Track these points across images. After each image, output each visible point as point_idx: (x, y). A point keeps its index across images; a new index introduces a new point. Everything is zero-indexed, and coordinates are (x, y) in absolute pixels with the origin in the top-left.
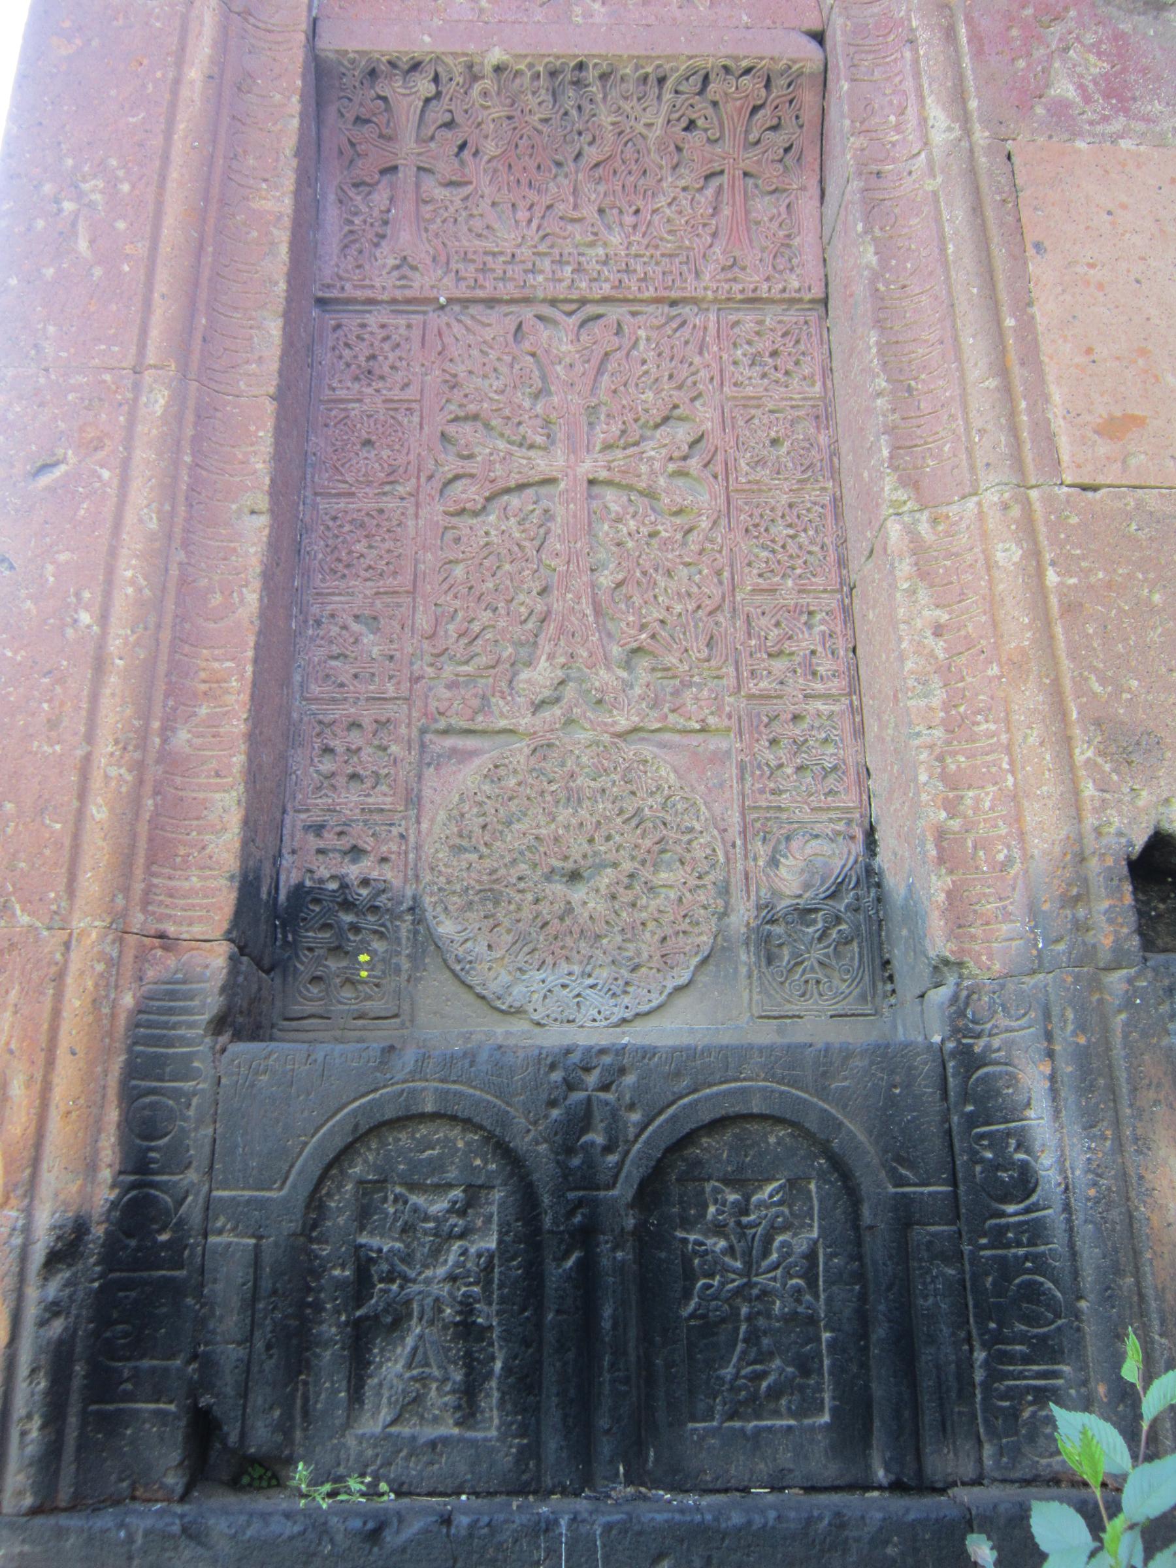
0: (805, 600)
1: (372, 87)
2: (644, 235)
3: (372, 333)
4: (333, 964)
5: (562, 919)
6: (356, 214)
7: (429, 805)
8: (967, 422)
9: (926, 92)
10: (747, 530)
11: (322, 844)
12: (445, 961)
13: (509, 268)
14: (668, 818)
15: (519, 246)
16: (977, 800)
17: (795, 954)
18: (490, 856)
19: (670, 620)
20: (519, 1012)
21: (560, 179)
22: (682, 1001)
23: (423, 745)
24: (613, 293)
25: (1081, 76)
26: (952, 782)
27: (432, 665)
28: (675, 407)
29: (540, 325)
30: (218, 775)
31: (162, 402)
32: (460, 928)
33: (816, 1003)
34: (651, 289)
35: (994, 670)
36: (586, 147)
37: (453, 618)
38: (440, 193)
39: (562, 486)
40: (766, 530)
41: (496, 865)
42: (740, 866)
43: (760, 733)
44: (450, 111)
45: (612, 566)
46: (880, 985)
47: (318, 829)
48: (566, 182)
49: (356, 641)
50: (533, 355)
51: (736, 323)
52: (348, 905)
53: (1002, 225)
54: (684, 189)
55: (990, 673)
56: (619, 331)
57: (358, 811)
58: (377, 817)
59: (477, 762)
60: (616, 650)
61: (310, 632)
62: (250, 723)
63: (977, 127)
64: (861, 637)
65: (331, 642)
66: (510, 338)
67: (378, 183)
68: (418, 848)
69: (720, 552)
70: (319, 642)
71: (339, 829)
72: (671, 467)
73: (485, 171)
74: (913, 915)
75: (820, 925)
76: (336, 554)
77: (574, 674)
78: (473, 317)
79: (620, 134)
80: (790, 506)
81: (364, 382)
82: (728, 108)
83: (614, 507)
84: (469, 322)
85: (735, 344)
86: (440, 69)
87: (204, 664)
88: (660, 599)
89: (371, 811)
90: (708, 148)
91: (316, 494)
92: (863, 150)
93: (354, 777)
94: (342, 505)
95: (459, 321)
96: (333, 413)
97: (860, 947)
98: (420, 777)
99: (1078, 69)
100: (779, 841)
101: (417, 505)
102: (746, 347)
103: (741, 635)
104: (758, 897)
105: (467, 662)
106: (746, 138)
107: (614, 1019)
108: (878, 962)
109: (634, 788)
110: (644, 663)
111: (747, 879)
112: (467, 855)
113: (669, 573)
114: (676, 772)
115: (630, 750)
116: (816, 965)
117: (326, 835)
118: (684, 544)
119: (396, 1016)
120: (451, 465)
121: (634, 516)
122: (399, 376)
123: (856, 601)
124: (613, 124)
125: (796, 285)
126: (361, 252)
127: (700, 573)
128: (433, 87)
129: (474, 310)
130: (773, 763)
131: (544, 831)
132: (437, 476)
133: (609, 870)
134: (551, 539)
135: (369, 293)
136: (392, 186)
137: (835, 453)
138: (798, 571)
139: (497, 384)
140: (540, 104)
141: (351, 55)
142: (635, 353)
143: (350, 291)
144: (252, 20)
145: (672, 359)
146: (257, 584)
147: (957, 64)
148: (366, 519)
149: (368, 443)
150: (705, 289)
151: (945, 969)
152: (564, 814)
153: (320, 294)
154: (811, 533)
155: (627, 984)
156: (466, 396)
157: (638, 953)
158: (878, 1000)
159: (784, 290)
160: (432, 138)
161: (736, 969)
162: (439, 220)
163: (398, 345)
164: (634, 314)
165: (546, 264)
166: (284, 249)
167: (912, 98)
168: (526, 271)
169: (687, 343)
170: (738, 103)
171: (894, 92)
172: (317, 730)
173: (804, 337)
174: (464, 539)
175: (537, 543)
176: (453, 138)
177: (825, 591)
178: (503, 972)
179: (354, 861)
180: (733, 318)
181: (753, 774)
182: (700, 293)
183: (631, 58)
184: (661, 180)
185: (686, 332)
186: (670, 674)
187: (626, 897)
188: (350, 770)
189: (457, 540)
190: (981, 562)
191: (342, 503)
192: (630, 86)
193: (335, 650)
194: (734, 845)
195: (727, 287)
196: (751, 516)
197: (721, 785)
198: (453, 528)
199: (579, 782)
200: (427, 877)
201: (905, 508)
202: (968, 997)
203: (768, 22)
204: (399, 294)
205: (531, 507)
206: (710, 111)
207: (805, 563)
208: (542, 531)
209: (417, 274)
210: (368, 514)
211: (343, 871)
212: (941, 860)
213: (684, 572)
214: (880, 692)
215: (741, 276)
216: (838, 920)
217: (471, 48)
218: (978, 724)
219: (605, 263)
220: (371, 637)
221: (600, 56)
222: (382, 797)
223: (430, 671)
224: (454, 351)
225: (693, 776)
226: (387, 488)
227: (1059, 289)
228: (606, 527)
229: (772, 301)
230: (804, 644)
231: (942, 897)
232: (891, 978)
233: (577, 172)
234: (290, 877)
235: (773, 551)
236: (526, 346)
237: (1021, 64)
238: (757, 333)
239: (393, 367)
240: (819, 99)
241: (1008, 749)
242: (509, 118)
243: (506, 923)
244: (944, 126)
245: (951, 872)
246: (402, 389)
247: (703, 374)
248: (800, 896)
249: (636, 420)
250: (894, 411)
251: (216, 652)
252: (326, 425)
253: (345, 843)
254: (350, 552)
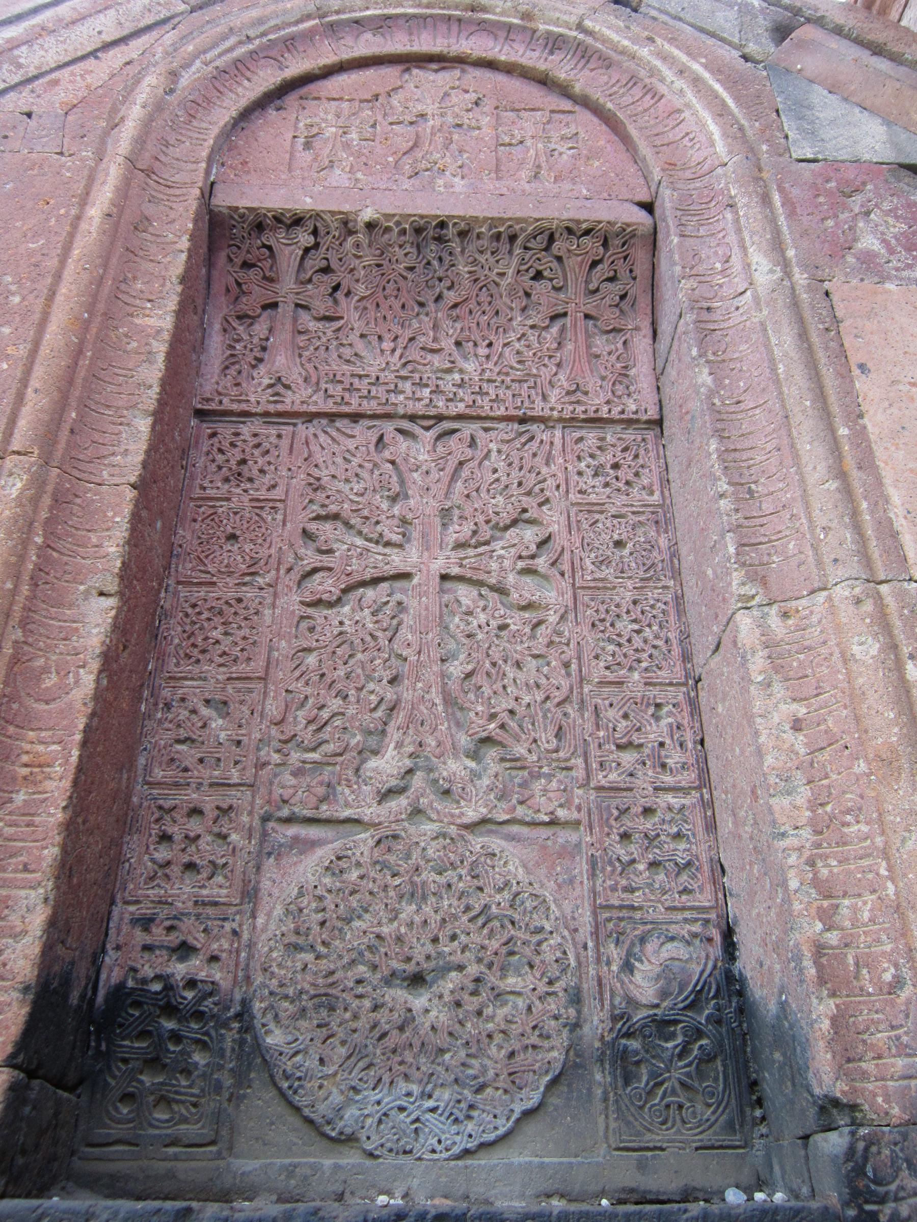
0: (652, 692)
1: (259, 238)
2: (495, 364)
3: (244, 441)
4: (147, 1079)
5: (401, 1029)
6: (238, 341)
7: (266, 899)
8: (810, 520)
9: (748, 244)
10: (593, 625)
11: (148, 940)
12: (272, 1077)
13: (373, 389)
14: (516, 917)
15: (383, 370)
16: (855, 910)
17: (653, 1075)
18: (326, 956)
19: (521, 710)
20: (348, 1140)
21: (422, 316)
22: (531, 1128)
23: (265, 834)
24: (467, 411)
25: (883, 233)
26: (825, 888)
27: (278, 751)
28: (525, 511)
29: (400, 438)
30: (26, 869)
31: (19, 485)
32: (290, 1038)
33: (679, 1132)
34: (503, 409)
35: (861, 767)
36: (445, 291)
37: (302, 705)
38: (312, 325)
39: (415, 581)
40: (612, 625)
41: (332, 967)
42: (592, 972)
43: (611, 827)
44: (327, 259)
45: (462, 657)
46: (748, 1110)
47: (146, 923)
48: (427, 319)
49: (204, 726)
50: (393, 463)
51: (581, 439)
52: (170, 1010)
53: (827, 348)
54: (532, 327)
55: (856, 770)
56: (473, 443)
57: (191, 904)
58: (210, 911)
59: (320, 852)
60: (463, 740)
61: (159, 715)
62: (69, 812)
63: (796, 270)
64: (710, 730)
65: (179, 726)
66: (372, 447)
67: (259, 316)
68: (251, 945)
69: (568, 644)
70: (167, 725)
71: (168, 923)
72: (520, 564)
73: (356, 308)
74: (789, 1039)
75: (680, 1039)
76: (192, 640)
77: (421, 762)
78: (338, 430)
79: (476, 280)
80: (635, 602)
81: (232, 483)
82: (571, 262)
83: (465, 601)
84: (334, 433)
85: (579, 458)
86: (318, 224)
87: (27, 747)
88: (509, 690)
89: (204, 904)
90: (553, 294)
91: (179, 583)
92: (693, 290)
93: (190, 866)
94: (202, 594)
95: (326, 432)
96: (203, 509)
97: (725, 1066)
98: (258, 868)
99: (881, 228)
100: (633, 944)
101: (275, 595)
102: (589, 460)
103: (589, 726)
104: (613, 1006)
105: (314, 749)
106: (586, 288)
107: (456, 1150)
108: (744, 1083)
109: (481, 884)
110: (491, 754)
111: (600, 984)
112: (303, 955)
113: (518, 665)
114: (525, 866)
115: (477, 842)
116: (677, 1086)
117: (154, 930)
118: (533, 637)
119: (213, 1143)
120: (311, 558)
121: (484, 609)
122: (267, 480)
123: (701, 694)
124: (470, 272)
125: (633, 408)
126: (240, 372)
127: (548, 664)
128: (312, 239)
129: (339, 424)
130: (625, 859)
131: (385, 930)
132: (296, 569)
133: (453, 974)
134: (403, 630)
135: (244, 407)
136: (272, 319)
137: (675, 554)
138: (644, 665)
139: (357, 487)
140: (406, 255)
141: (242, 211)
142: (487, 463)
143: (227, 404)
144: (155, 177)
145: (521, 469)
146: (95, 665)
147: (773, 221)
148: (224, 607)
149: (233, 537)
150: (552, 409)
151: (835, 1111)
152: (408, 910)
153: (199, 406)
154: (655, 628)
155: (471, 1107)
156: (328, 497)
157: (484, 1070)
158: (747, 1128)
159: (623, 412)
160: (310, 281)
161: (589, 1090)
162: (312, 348)
163: (268, 452)
164: (486, 430)
165: (407, 386)
166: (161, 358)
167: (736, 250)
168: (388, 391)
169: (535, 455)
170: (580, 258)
171: (718, 245)
172: (157, 815)
173: (642, 452)
174: (318, 629)
175: (389, 634)
176: (330, 280)
177: (671, 684)
178: (335, 1090)
179: (182, 959)
180: (577, 434)
181: (603, 870)
182: (547, 413)
183: (486, 219)
184: (511, 320)
185: (534, 445)
186: (518, 764)
187: (472, 1003)
188: (186, 859)
189: (312, 629)
190: (837, 655)
191: (202, 592)
192: (485, 242)
193: (183, 734)
194: (585, 947)
195: (571, 408)
196: (597, 611)
197: (571, 881)
198: (309, 617)
199: (424, 876)
200: (258, 979)
201: (753, 603)
202: (866, 1149)
203: (605, 195)
204: (271, 408)
205: (385, 600)
206: (555, 265)
207: (651, 656)
208: (395, 622)
209: (290, 393)
210: (227, 603)
211: (169, 971)
212: (822, 980)
213: (533, 664)
214: (734, 786)
215: (583, 398)
216: (699, 1033)
217: (346, 208)
218: (848, 824)
219: (460, 386)
220: (220, 722)
221: (459, 217)
222: (218, 889)
223: (276, 758)
224: (319, 458)
225: (542, 871)
226: (247, 579)
227: (886, 404)
228: (457, 620)
229: (612, 421)
230: (652, 736)
231: (826, 1024)
232: (759, 1102)
233: (436, 312)
234: (112, 973)
235: (619, 645)
236: (387, 454)
237: (830, 223)
238: (599, 448)
239: (262, 471)
240: (649, 256)
241: (885, 854)
242: (378, 266)
243: (341, 1034)
244: (766, 269)
245: (833, 994)
246: (269, 490)
247: (551, 482)
248: (657, 1006)
249: (487, 522)
250: (737, 510)
251: (43, 734)
252: (195, 520)
253: (174, 939)
254: (206, 639)
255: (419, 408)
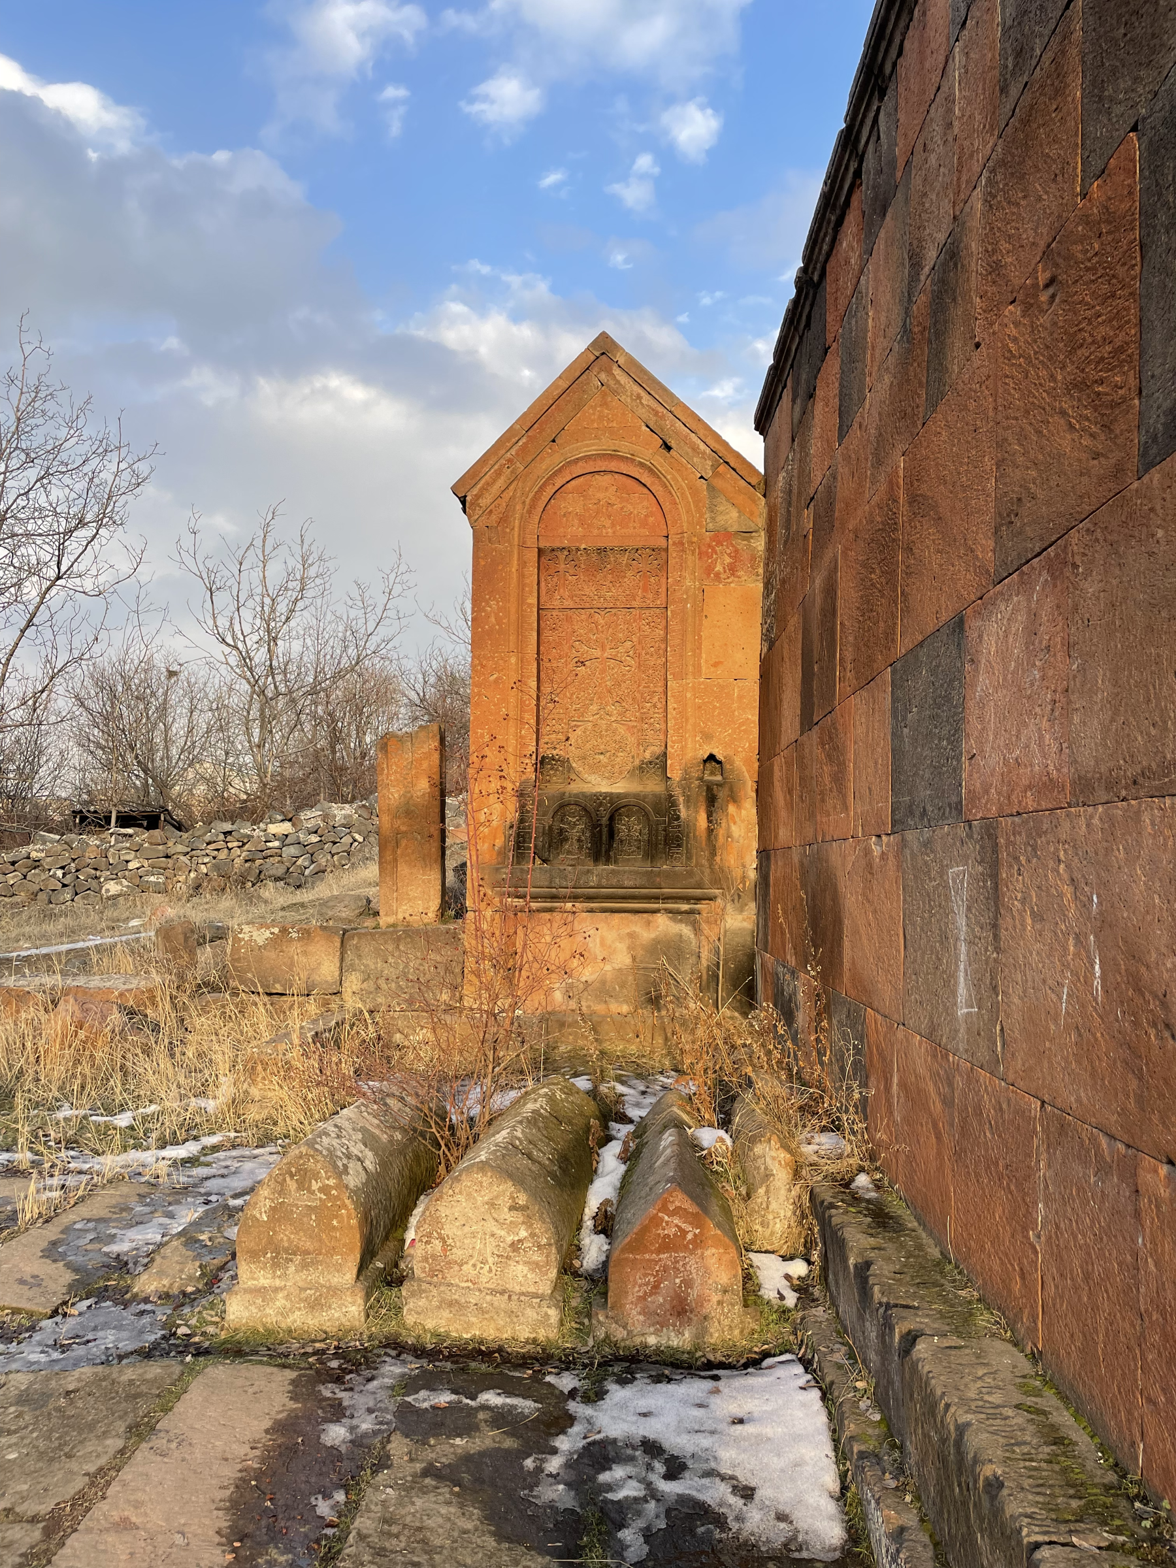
255: (600, 605)
